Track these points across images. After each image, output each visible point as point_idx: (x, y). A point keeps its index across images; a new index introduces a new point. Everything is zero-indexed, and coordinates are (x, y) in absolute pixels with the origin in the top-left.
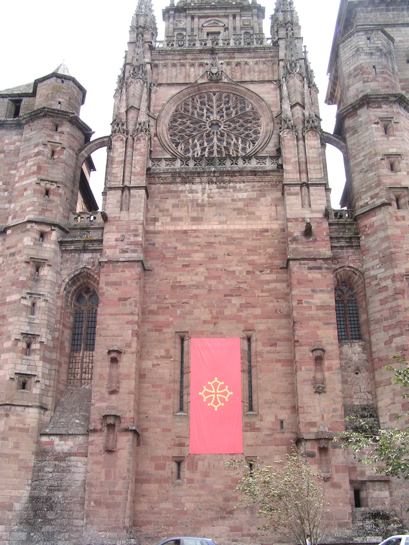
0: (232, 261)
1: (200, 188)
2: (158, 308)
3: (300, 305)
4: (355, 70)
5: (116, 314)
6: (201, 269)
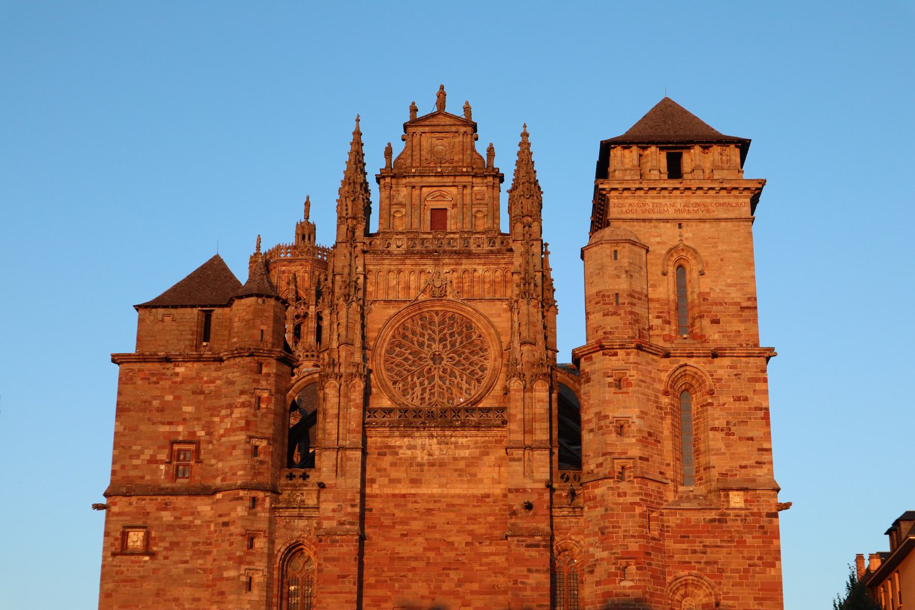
0: (451, 531)
1: (420, 443)
2: (376, 581)
3: (515, 586)
4: (598, 294)
5: (335, 593)
6: (420, 539)
